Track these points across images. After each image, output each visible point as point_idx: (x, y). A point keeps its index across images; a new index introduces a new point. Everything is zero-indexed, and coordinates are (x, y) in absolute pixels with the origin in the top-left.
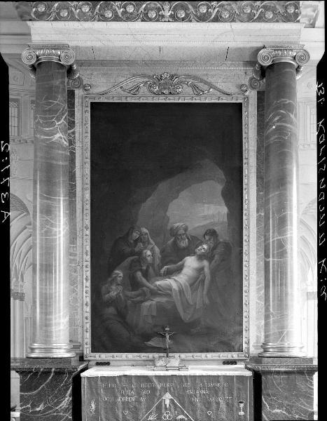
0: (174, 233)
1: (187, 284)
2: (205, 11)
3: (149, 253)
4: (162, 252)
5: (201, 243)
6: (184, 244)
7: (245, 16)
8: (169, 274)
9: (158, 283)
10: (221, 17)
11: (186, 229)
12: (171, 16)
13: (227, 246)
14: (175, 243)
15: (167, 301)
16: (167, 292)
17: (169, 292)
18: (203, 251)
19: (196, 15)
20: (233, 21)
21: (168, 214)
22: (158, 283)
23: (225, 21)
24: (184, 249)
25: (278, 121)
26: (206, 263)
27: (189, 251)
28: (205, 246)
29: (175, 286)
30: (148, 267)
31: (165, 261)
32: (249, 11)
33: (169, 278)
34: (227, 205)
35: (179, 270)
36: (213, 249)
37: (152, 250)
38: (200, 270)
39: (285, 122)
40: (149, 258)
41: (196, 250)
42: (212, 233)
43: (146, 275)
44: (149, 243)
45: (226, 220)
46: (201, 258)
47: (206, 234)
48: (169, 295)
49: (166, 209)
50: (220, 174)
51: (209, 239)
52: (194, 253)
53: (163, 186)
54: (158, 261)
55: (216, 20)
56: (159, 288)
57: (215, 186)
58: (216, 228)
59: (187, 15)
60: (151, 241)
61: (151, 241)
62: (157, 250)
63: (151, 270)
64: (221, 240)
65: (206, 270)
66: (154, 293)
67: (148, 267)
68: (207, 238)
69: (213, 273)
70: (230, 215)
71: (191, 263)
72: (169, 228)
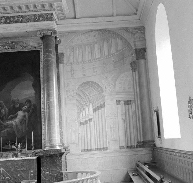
0: (13, 102)
1: (19, 123)
2: (17, 19)
3: (3, 111)
4: (9, 110)
5: (24, 105)
6: (17, 106)
7: (32, 20)
8: (12, 119)
9: (7, 123)
10: (23, 21)
11: (18, 100)
12: (4, 22)
13: (35, 106)
14: (14, 106)
15: (11, 130)
16: (11, 126)
17: (12, 126)
18: (25, 108)
19: (14, 21)
20: (28, 22)
21: (11, 95)
22: (7, 123)
23: (24, 22)
24: (18, 108)
25: (46, 57)
26: (26, 113)
27: (19, 109)
28: (26, 107)
29: (14, 123)
30: (3, 117)
31: (9, 114)
32: (34, 18)
33: (12, 120)
34: (35, 89)
35: (16, 117)
36: (29, 108)
37: (5, 109)
38: (24, 116)
39: (49, 57)
40: (4, 113)
41: (23, 108)
42: (29, 101)
43: (2, 120)
44: (4, 107)
45: (34, 95)
46: (24, 111)
47: (26, 101)
48: (12, 127)
49: (10, 93)
50: (32, 78)
51: (28, 104)
52: (22, 110)
53: (9, 84)
54: (7, 114)
55: (21, 22)
56: (8, 125)
57: (29, 83)
58: (30, 99)
59: (10, 21)
60: (4, 106)
61: (4, 106)
62: (7, 109)
63: (4, 118)
64: (32, 104)
65: (27, 116)
66: (6, 127)
67: (3, 117)
68: (27, 103)
69: (29, 117)
70: (36, 94)
71: (20, 114)
72: (11, 100)
